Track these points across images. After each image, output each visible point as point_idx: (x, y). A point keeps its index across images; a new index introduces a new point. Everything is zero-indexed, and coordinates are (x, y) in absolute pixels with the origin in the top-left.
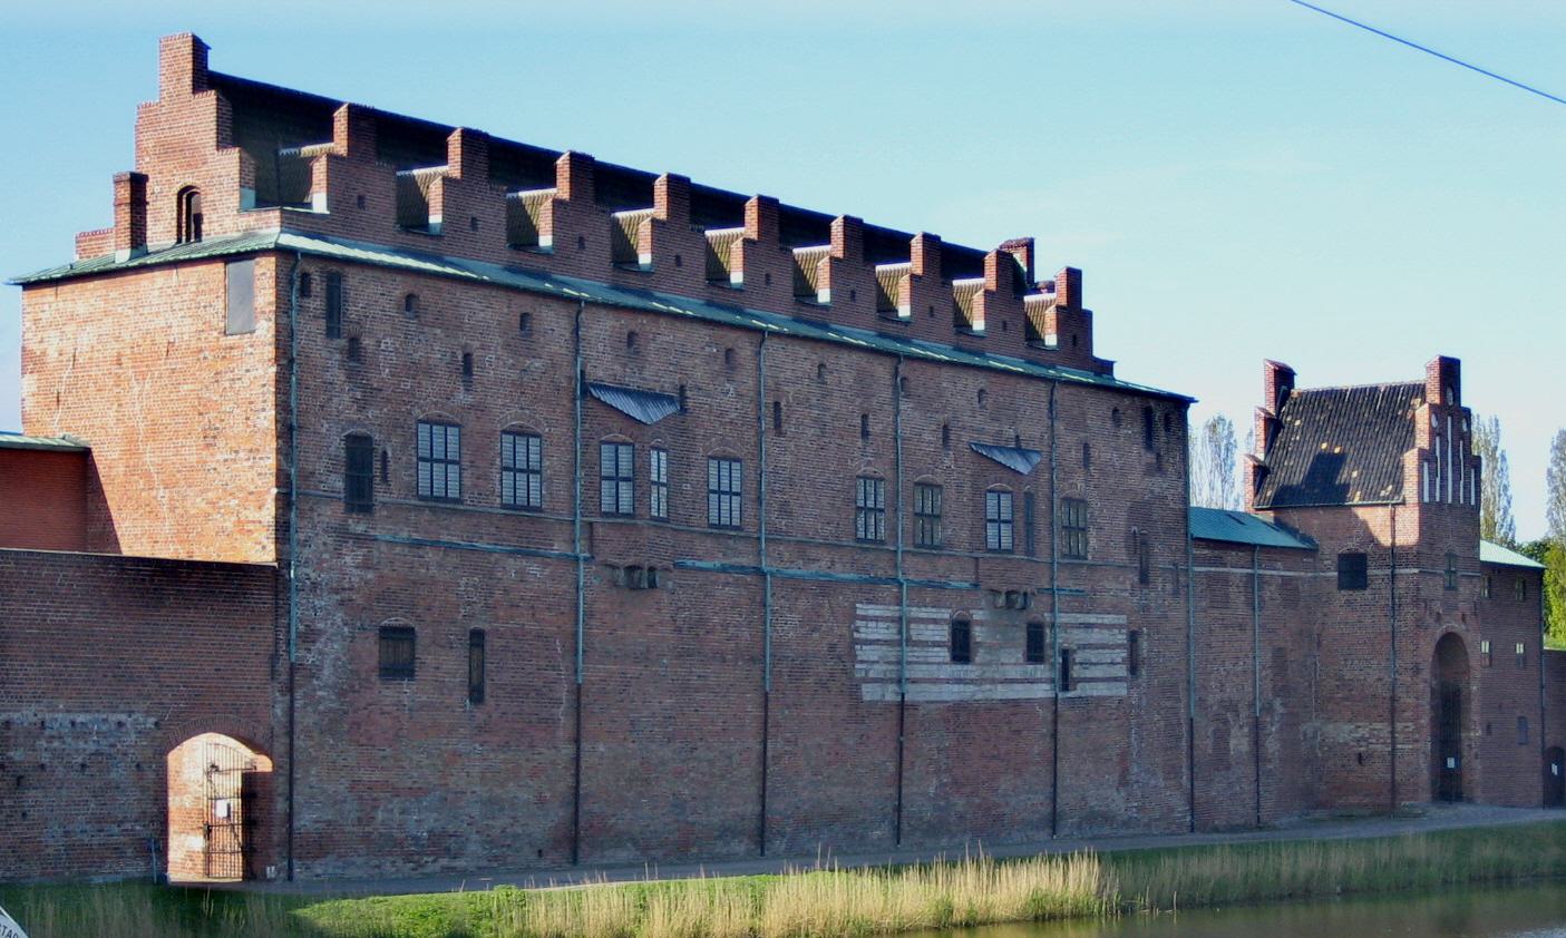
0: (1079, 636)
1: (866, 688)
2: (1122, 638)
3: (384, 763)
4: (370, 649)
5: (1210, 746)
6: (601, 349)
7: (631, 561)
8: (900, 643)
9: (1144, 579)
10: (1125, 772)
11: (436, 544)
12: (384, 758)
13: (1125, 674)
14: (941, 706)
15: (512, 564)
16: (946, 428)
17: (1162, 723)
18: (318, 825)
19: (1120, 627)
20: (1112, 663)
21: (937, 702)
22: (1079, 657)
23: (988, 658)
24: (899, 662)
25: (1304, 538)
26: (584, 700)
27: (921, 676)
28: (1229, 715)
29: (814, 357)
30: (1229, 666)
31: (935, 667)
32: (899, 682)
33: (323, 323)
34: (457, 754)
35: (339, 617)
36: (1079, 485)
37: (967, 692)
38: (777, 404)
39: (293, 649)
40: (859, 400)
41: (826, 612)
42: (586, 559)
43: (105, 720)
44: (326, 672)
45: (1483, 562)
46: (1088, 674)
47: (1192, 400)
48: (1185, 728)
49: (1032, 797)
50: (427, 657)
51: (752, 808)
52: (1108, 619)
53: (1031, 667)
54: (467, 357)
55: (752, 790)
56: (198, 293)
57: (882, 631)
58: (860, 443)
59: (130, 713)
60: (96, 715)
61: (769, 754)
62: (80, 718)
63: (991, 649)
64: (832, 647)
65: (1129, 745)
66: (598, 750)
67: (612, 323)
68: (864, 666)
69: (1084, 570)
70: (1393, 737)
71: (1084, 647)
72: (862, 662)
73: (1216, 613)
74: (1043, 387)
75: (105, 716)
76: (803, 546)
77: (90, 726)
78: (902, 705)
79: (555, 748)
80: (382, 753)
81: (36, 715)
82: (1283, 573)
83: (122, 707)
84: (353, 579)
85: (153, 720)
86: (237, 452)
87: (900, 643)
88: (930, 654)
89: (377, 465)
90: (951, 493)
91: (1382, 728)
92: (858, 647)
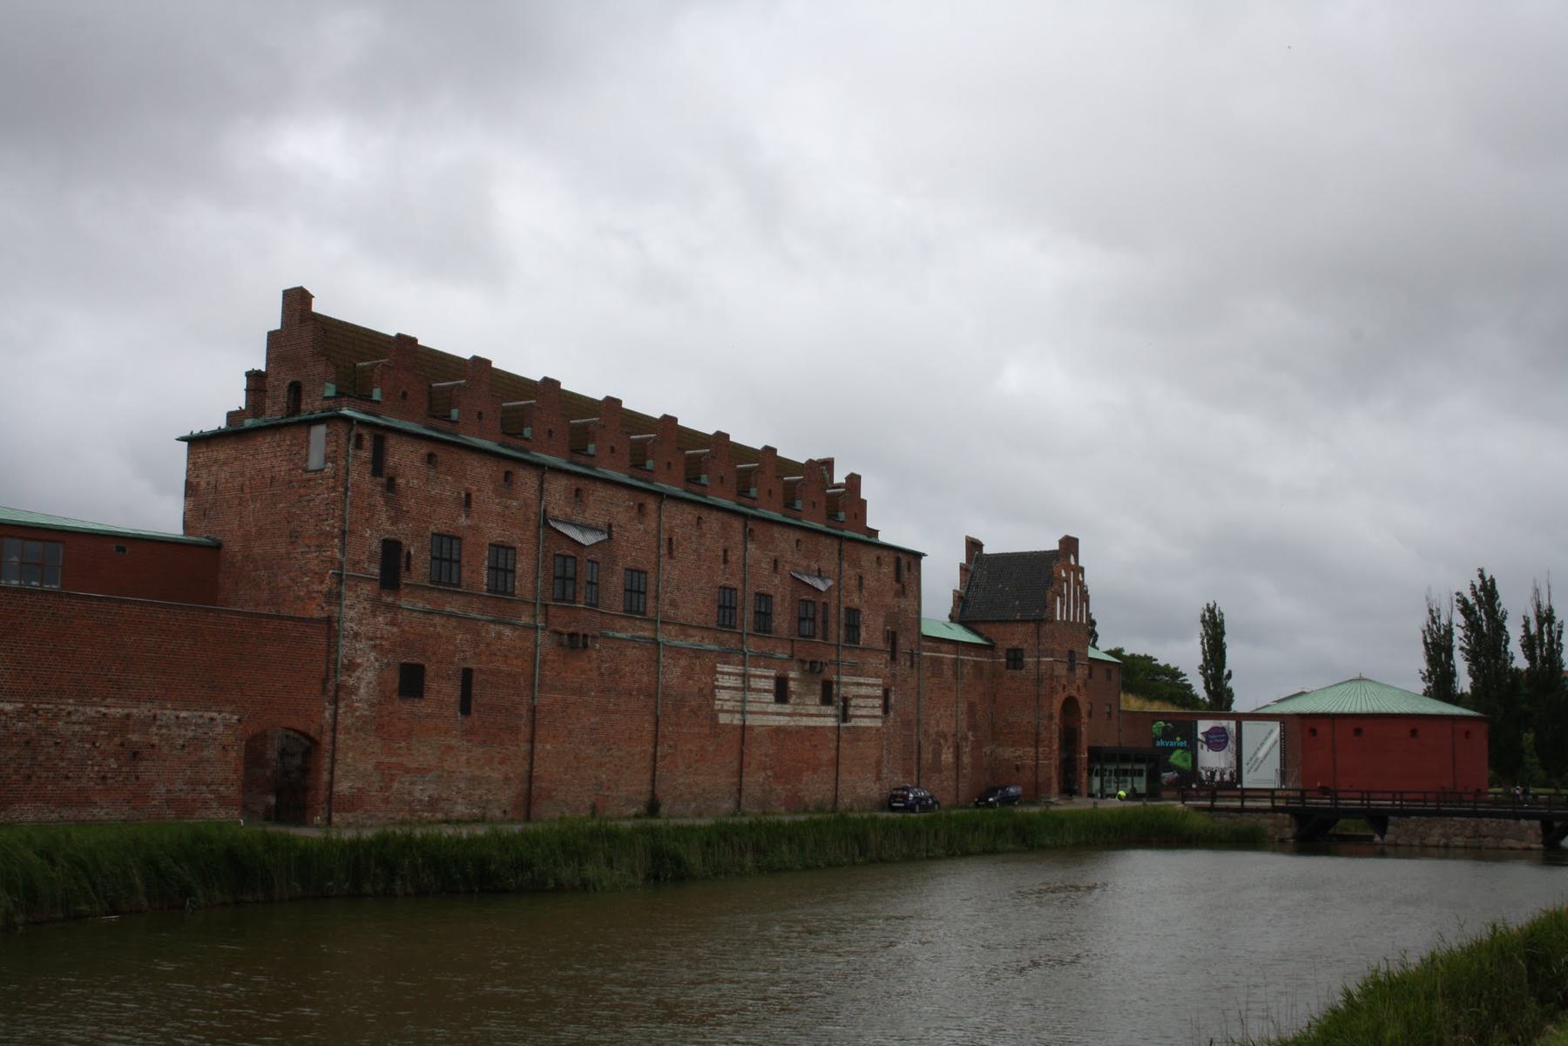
0: (854, 690)
1: (720, 715)
2: (879, 692)
3: (400, 752)
6: (558, 498)
7: (571, 630)
8: (743, 689)
9: (893, 658)
10: (879, 772)
11: (441, 614)
12: (400, 748)
15: (492, 626)
16: (776, 561)
17: (901, 744)
18: (350, 791)
19: (878, 685)
20: (874, 707)
22: (853, 702)
23: (798, 701)
24: (743, 701)
25: (986, 640)
26: (537, 716)
28: (942, 741)
29: (695, 512)
30: (942, 711)
31: (765, 705)
32: (743, 713)
33: (370, 467)
34: (450, 748)
35: (372, 656)
36: (856, 601)
37: (783, 721)
38: (670, 540)
39: (339, 676)
40: (722, 541)
41: (698, 669)
42: (543, 629)
43: (201, 717)
44: (362, 691)
45: (1091, 658)
47: (924, 555)
48: (916, 747)
50: (432, 684)
51: (646, 788)
52: (871, 681)
53: (823, 708)
54: (468, 495)
55: (647, 777)
56: (291, 445)
58: (722, 567)
59: (220, 712)
60: (195, 713)
61: (659, 754)
62: (183, 714)
63: (800, 695)
64: (701, 690)
65: (882, 756)
66: (546, 747)
67: (566, 482)
68: (720, 702)
69: (858, 651)
70: (1037, 757)
72: (720, 700)
74: (836, 544)
75: (201, 713)
76: (685, 628)
77: (190, 719)
78: (743, 727)
79: (517, 745)
80: (397, 745)
81: (149, 711)
82: (975, 659)
83: (214, 708)
84: (384, 631)
85: (236, 717)
86: (309, 547)
87: (743, 689)
89: (403, 560)
90: (777, 599)
91: (1031, 751)
92: (717, 690)
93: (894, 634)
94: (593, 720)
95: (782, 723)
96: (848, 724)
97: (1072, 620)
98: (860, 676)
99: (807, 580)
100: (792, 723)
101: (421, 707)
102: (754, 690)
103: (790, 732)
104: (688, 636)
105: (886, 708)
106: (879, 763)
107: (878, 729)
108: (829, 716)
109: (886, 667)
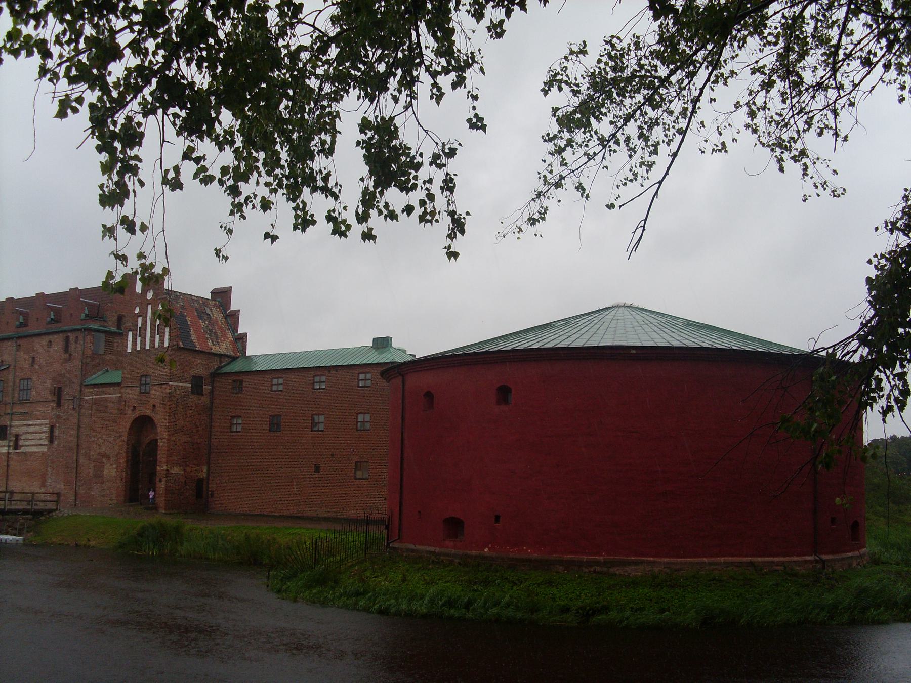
0: (24, 429)
2: (46, 429)
5: (91, 473)
9: (59, 405)
13: (47, 443)
19: (46, 424)
20: (41, 439)
28: (104, 460)
46: (27, 443)
52: (38, 422)
65: (47, 471)
69: (28, 405)
71: (26, 433)
73: (99, 416)
93: (60, 388)
96: (18, 451)
97: (148, 347)
98: (29, 420)
105: (51, 439)
106: (43, 477)
107: (43, 453)
109: (52, 411)
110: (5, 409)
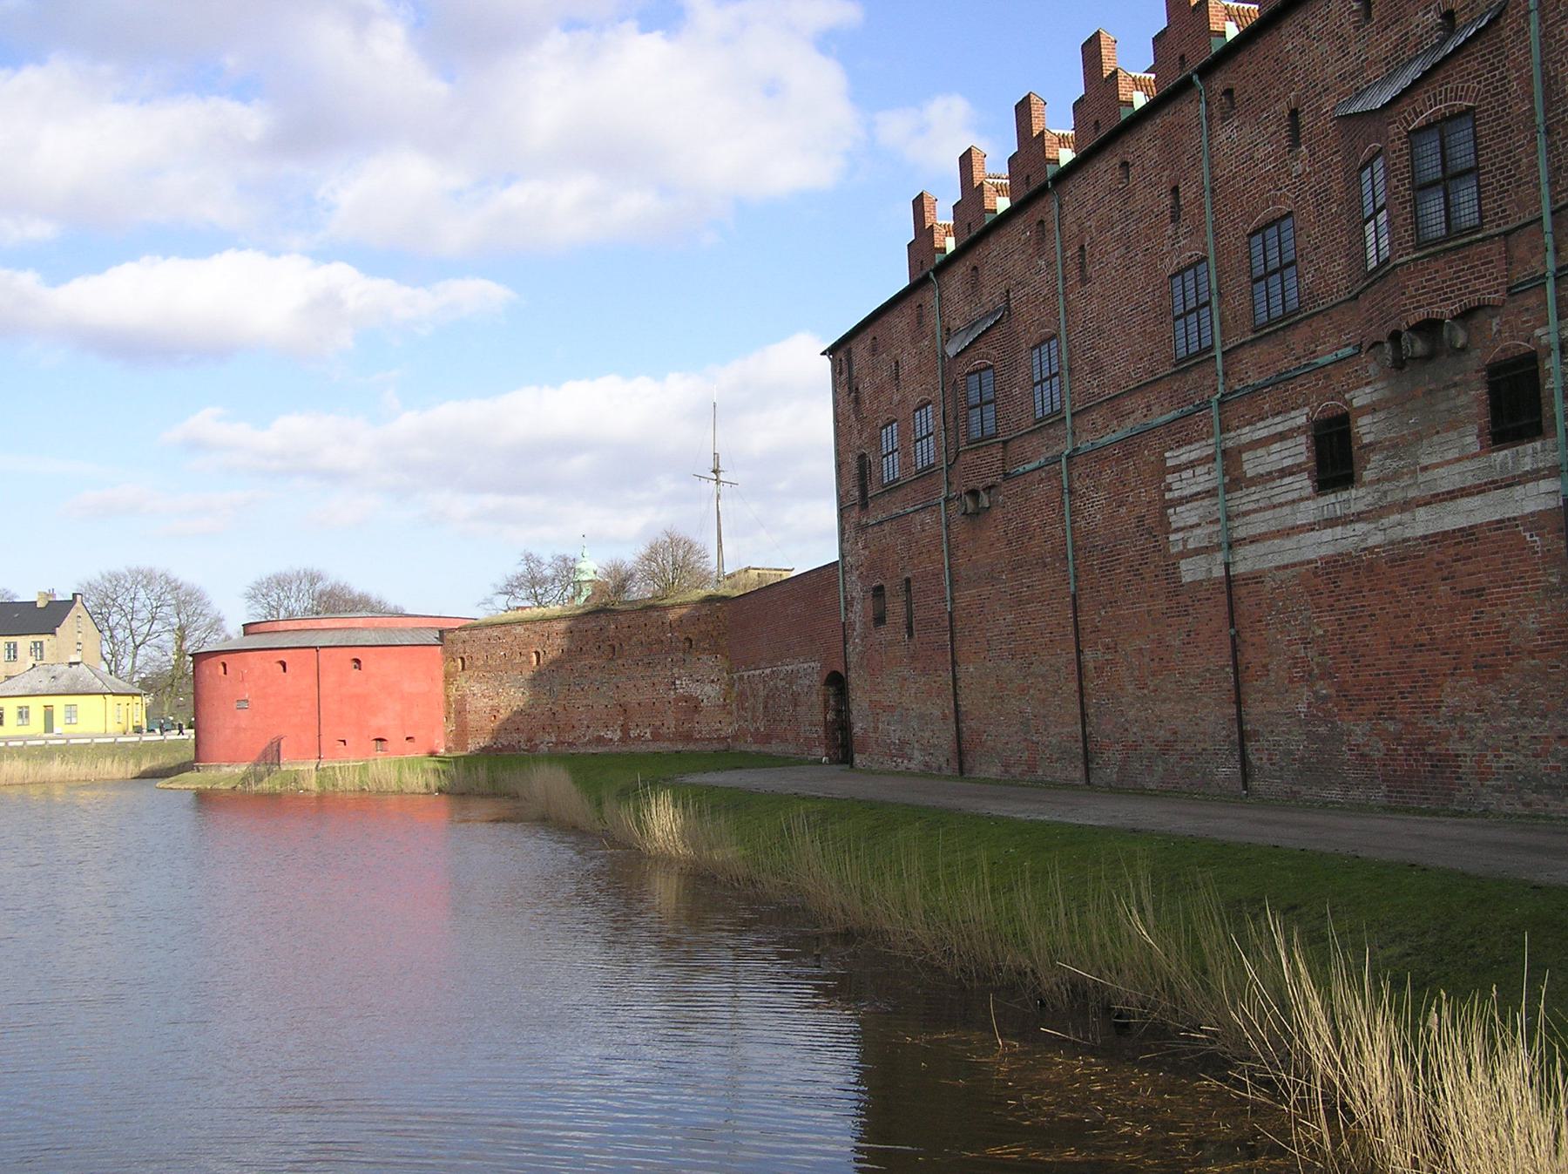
1: (1184, 565)
4: (869, 602)
14: (1303, 569)
16: (1294, 113)
21: (1294, 565)
27: (1264, 529)
31: (1287, 510)
38: (1082, 247)
49: (1531, 722)
53: (1502, 456)
57: (1201, 479)
63: (1395, 448)
64: (1141, 519)
66: (968, 669)
68: (1180, 535)
72: (1178, 530)
78: (1229, 579)
88: (1277, 491)
92: (1171, 511)
94: (1010, 617)
95: (1341, 547)
99: (1357, 107)
100: (1376, 539)
101: (884, 634)
102: (1253, 481)
103: (1371, 567)
104: (1121, 417)
108: (1535, 475)
110: (1509, 260)
